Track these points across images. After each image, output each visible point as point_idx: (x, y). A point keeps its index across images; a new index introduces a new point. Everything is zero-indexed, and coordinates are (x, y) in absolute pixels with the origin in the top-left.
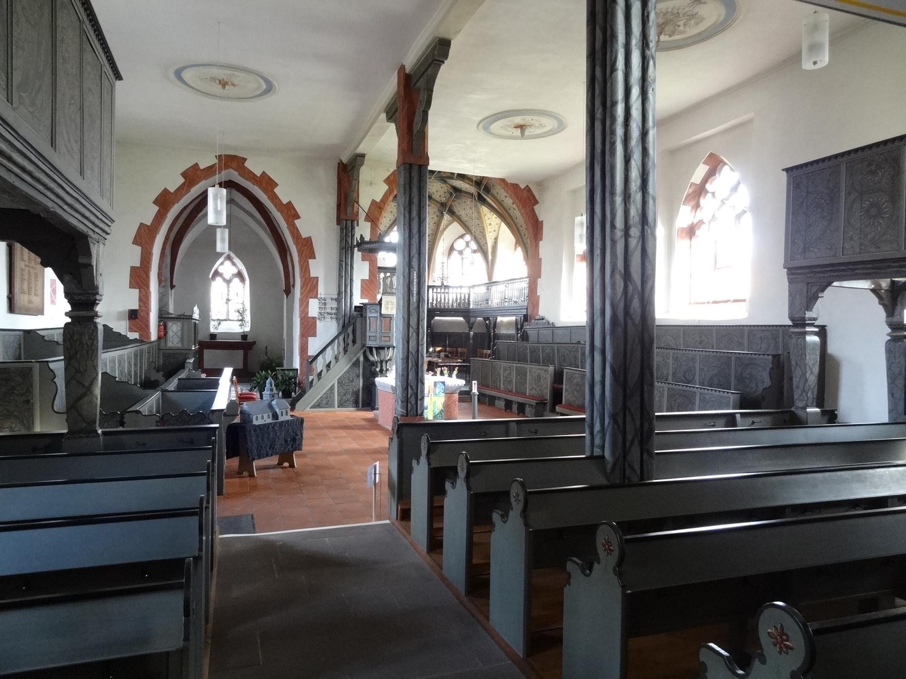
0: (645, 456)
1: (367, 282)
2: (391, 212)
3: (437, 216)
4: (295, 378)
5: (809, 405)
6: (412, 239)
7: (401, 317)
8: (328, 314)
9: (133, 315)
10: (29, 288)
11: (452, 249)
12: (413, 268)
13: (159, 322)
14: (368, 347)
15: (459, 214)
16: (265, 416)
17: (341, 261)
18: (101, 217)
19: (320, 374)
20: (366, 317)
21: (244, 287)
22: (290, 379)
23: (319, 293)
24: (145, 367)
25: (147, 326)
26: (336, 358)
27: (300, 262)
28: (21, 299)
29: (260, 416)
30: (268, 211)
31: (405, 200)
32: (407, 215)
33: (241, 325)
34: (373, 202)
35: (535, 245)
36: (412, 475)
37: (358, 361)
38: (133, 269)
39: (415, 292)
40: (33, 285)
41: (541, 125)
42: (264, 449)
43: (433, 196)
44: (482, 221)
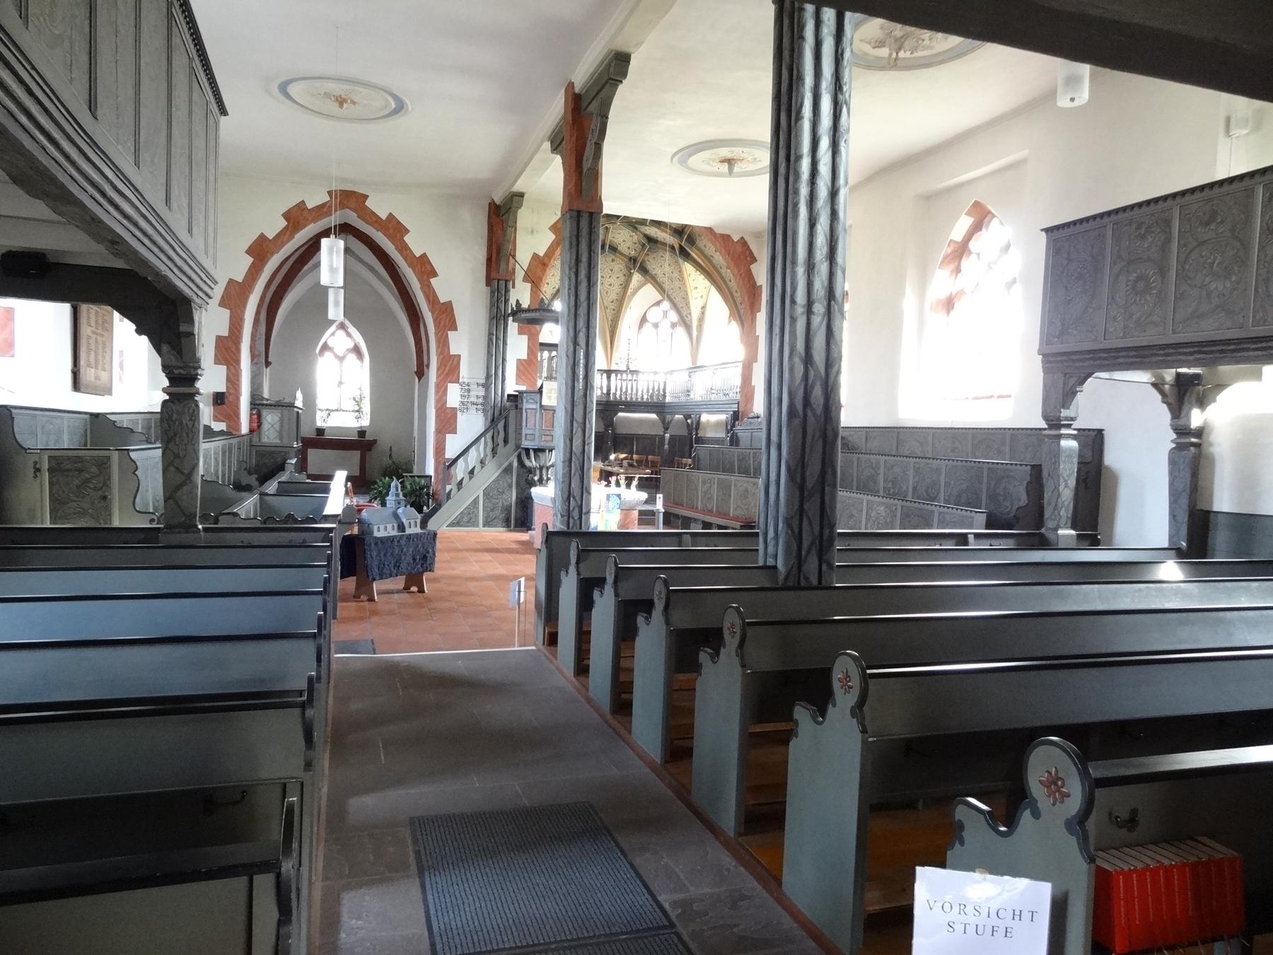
0: (824, 567)
1: (524, 363)
3: (624, 275)
4: (428, 487)
5: (1062, 526)
6: (579, 307)
7: (563, 408)
8: (473, 404)
9: (219, 399)
10: (97, 361)
11: (644, 320)
12: (578, 345)
13: (251, 410)
14: (523, 448)
15: (654, 273)
16: (389, 527)
17: (490, 334)
18: (205, 278)
19: (460, 483)
20: (521, 409)
21: (362, 367)
22: (422, 488)
23: (461, 376)
24: (234, 468)
25: (237, 415)
26: (482, 462)
27: (436, 334)
28: (88, 375)
29: (382, 527)
30: (395, 265)
31: (571, 258)
32: (573, 276)
33: (357, 418)
34: (535, 256)
35: (751, 317)
36: (561, 589)
37: (510, 465)
39: (581, 377)
40: (100, 358)
41: (755, 159)
42: (387, 566)
43: (619, 248)
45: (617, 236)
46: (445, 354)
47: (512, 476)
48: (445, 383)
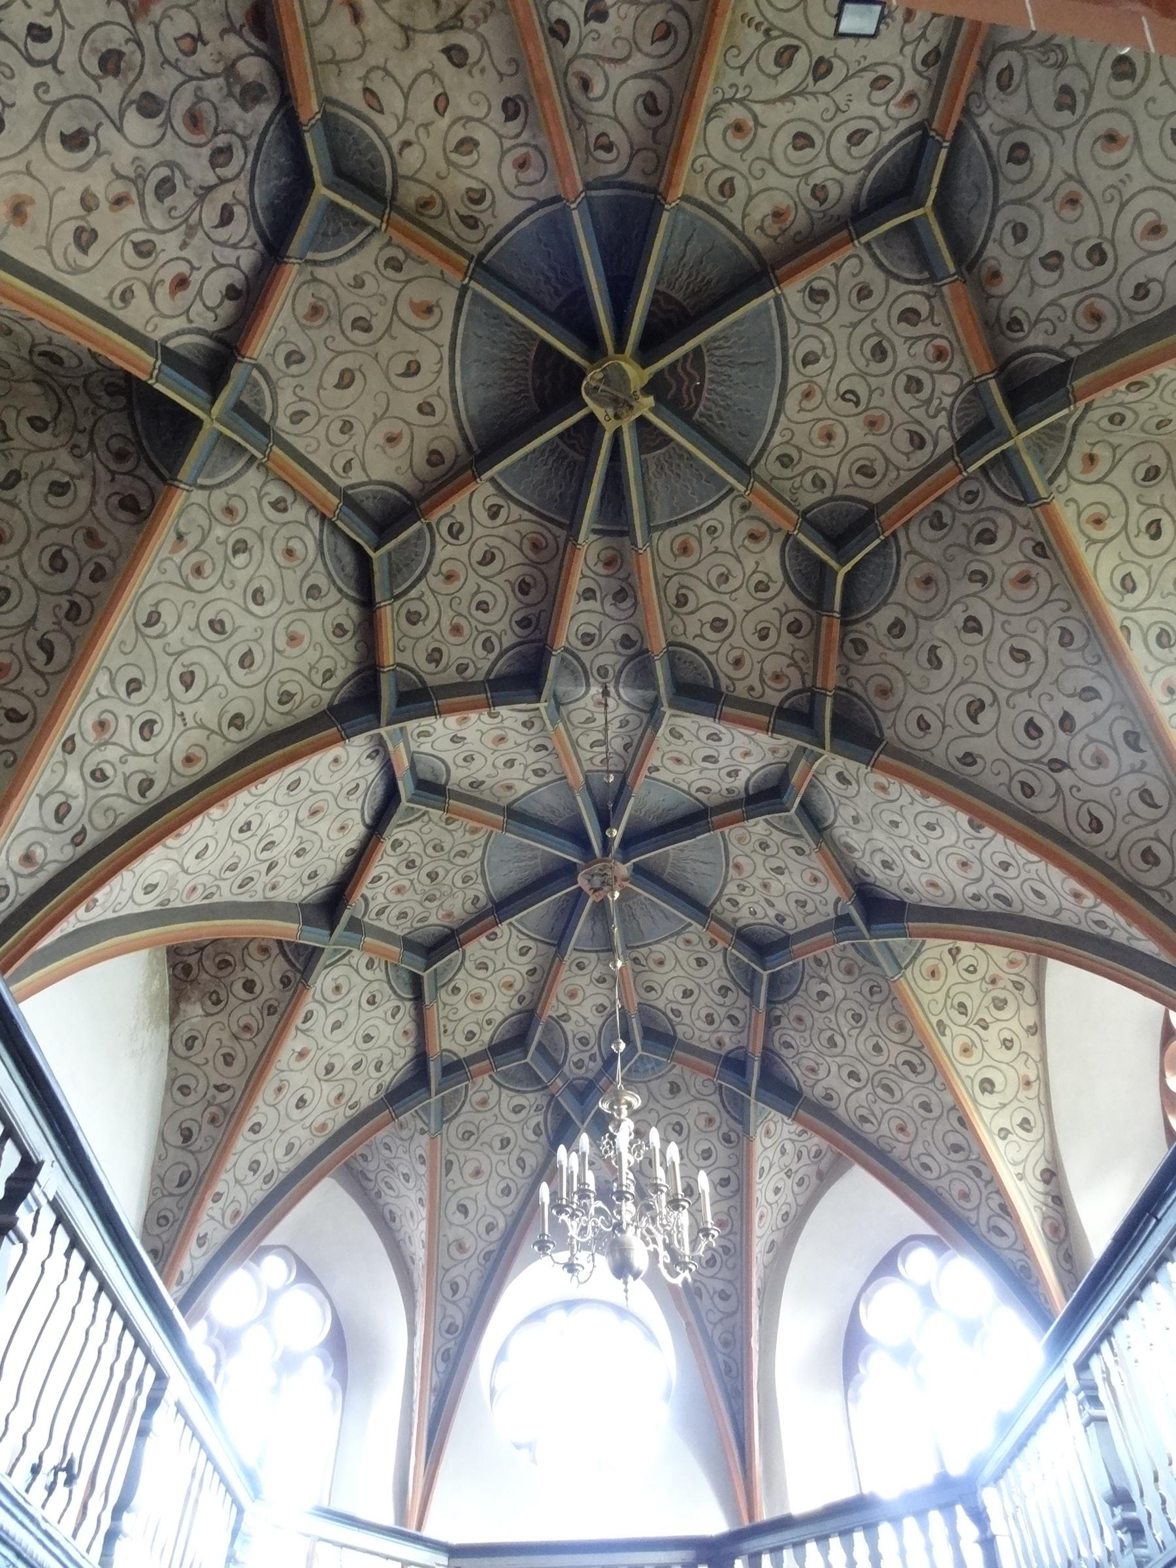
2: (505, 1143)
3: (727, 1139)
15: (819, 1091)
44: (938, 1070)
45: (657, 977)
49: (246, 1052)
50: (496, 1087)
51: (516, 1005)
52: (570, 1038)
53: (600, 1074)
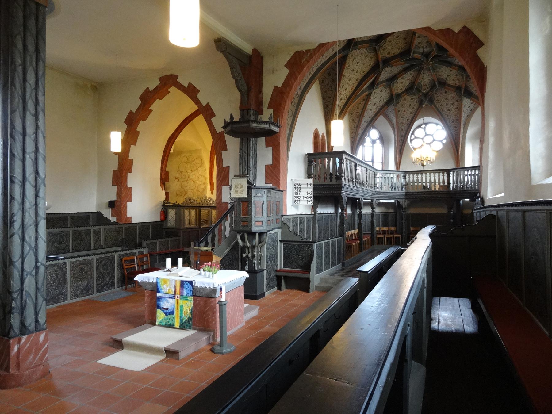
1: (271, 168)
3: (457, 101)
9: (111, 204)
34: (276, 88)
38: (114, 171)
43: (447, 82)
46: (221, 166)
47: (238, 252)
48: (220, 187)
49: (361, 107)
50: (407, 96)
51: (410, 82)
52: (422, 85)
53: (429, 91)
